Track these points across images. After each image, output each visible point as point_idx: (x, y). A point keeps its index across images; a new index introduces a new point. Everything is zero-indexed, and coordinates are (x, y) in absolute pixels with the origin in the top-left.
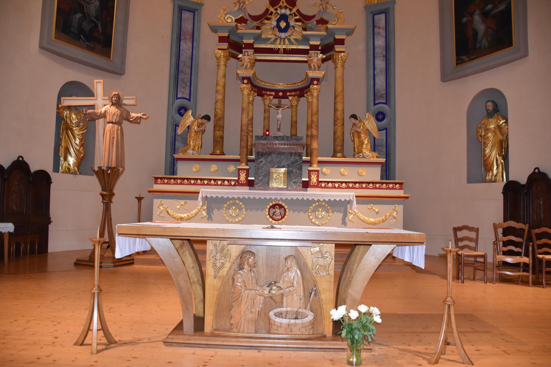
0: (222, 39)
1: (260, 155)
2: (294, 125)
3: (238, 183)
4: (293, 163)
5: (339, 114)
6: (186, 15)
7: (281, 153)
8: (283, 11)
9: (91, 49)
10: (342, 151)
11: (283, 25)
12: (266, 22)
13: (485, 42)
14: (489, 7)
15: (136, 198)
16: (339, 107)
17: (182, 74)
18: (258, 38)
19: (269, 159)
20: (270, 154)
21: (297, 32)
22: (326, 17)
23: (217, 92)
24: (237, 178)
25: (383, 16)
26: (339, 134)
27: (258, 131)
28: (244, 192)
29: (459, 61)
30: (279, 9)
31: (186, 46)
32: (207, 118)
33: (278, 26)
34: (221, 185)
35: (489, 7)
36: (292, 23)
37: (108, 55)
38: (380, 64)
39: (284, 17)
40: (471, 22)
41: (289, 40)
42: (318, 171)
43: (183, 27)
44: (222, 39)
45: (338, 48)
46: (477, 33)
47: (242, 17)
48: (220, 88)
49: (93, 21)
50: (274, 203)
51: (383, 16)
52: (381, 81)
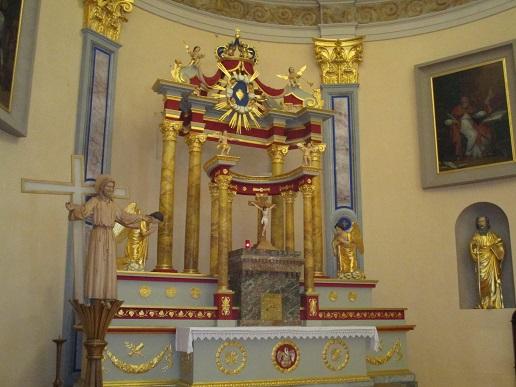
0: (169, 104)
3: (217, 315)
6: (101, 57)
7: (274, 273)
11: (240, 95)
13: (477, 151)
14: (481, 113)
15: (55, 341)
18: (210, 108)
20: (260, 273)
23: (163, 178)
24: (216, 308)
25: (346, 99)
29: (443, 168)
30: (235, 73)
31: (99, 102)
33: (234, 95)
34: (193, 318)
35: (481, 113)
36: (252, 95)
39: (241, 85)
40: (458, 126)
43: (96, 75)
46: (467, 140)
50: (280, 343)
51: (346, 99)
52: (343, 179)
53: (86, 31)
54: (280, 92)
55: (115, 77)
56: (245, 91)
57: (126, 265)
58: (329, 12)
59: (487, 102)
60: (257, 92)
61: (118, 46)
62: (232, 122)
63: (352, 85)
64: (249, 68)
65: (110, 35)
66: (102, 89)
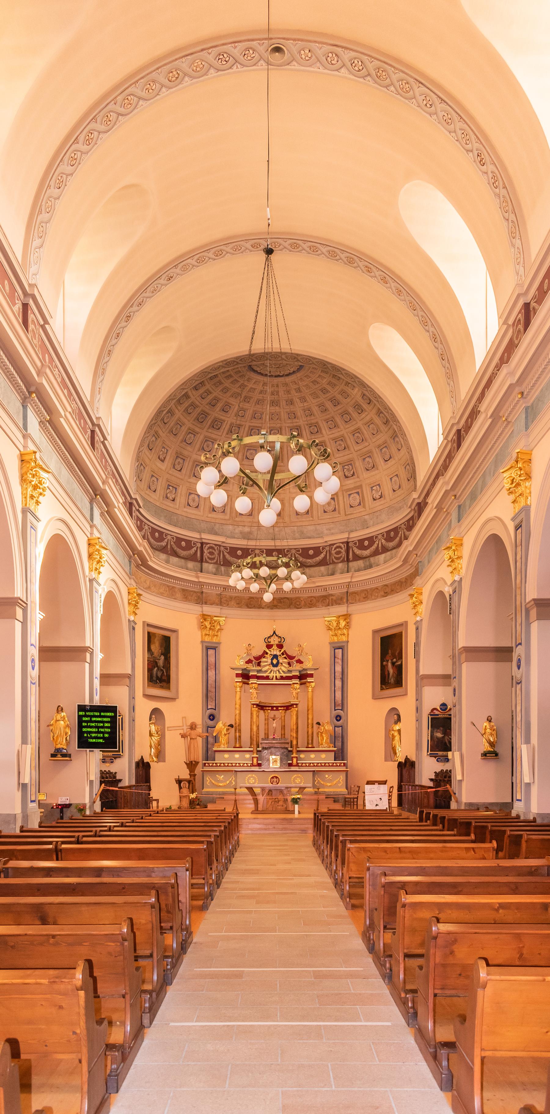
0: (238, 675)
1: (264, 748)
2: (283, 727)
3: (252, 765)
4: (283, 753)
5: (310, 721)
6: (211, 652)
8: (275, 653)
9: (162, 687)
10: (312, 743)
12: (264, 660)
13: (392, 681)
14: (395, 660)
16: (310, 717)
17: (210, 693)
19: (270, 751)
21: (284, 668)
22: (302, 660)
26: (310, 733)
27: (262, 735)
28: (256, 769)
31: (211, 673)
32: (231, 726)
35: (395, 660)
36: (281, 661)
37: (168, 688)
38: (338, 683)
39: (275, 657)
40: (387, 665)
41: (279, 671)
42: (297, 757)
44: (238, 675)
45: (309, 680)
47: (250, 660)
48: (238, 706)
49: (162, 670)
51: (341, 650)
52: (339, 695)
53: (202, 642)
54: (294, 657)
55: (219, 659)
56: (277, 659)
57: (219, 746)
58: (334, 598)
59: (397, 654)
60: (285, 658)
61: (219, 643)
62: (271, 675)
63: (343, 642)
64: (280, 646)
65: (215, 640)
66: (213, 667)
